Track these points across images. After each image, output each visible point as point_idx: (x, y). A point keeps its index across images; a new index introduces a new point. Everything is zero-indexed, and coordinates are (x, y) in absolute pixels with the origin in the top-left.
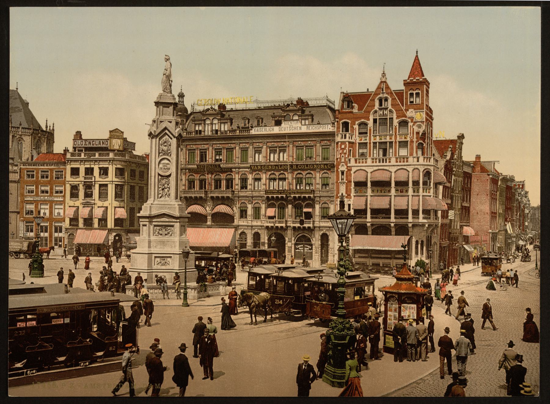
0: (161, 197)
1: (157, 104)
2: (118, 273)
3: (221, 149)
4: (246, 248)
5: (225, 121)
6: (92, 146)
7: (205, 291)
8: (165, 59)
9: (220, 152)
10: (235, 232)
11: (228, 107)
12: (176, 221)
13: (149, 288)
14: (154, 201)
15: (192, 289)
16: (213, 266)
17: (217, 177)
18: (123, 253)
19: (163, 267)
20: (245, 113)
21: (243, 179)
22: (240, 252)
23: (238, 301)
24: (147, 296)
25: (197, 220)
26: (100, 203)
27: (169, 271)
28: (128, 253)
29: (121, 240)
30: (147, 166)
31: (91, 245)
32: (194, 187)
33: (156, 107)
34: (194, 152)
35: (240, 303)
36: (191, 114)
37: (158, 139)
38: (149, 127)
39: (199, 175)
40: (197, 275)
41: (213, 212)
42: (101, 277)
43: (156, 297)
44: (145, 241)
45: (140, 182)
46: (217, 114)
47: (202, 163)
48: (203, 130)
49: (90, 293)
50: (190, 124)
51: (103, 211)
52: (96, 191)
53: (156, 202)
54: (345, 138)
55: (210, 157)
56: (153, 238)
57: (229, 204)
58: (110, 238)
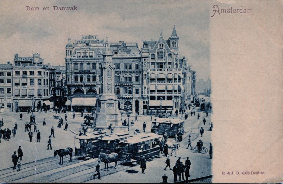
54: (146, 60)
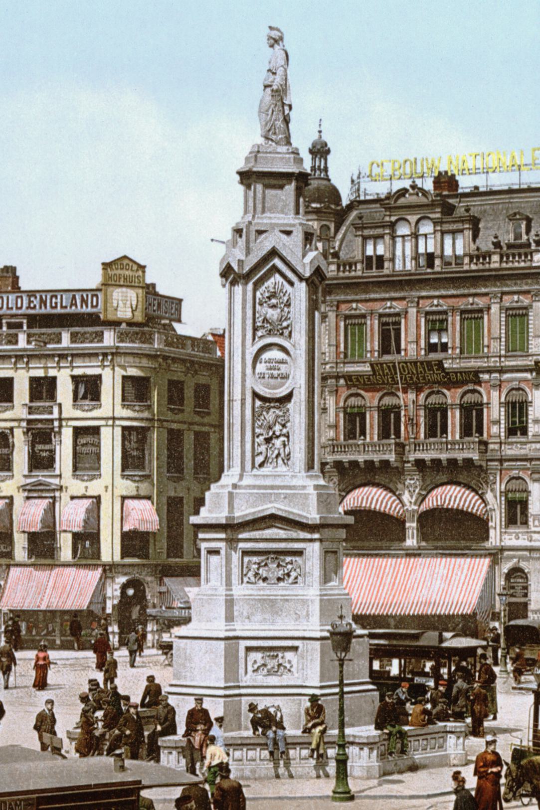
0: (262, 465)
1: (247, 177)
2: (136, 698)
3: (445, 313)
4: (526, 617)
5: (455, 227)
6: (49, 310)
7: (403, 752)
8: (270, 38)
9: (442, 321)
10: (492, 567)
11: (465, 183)
12: (309, 536)
13: (230, 745)
14: (241, 477)
15: (362, 745)
16: (426, 675)
17: (433, 399)
18: (149, 637)
19: (274, 680)
20: (517, 199)
21: (514, 404)
22: (507, 629)
23: (503, 781)
24: (223, 769)
25: (372, 533)
26: (76, 486)
27: (290, 692)
28: (166, 637)
29: (144, 597)
30: (218, 368)
31: (51, 614)
32: (363, 433)
33: (241, 188)
34: (361, 325)
35: (510, 788)
36: (351, 207)
37: (250, 286)
38: (221, 250)
39: (378, 395)
40: (377, 704)
41: (424, 508)
42: (84, 713)
43: (253, 771)
44: (216, 600)
45: (197, 419)
46: (431, 206)
47: (387, 358)
48: (388, 255)
49: (52, 763)
50: (350, 236)
51: (88, 511)
52: (64, 448)
53: (244, 482)
55: (412, 337)
56: (239, 590)
57: (473, 484)
58: (109, 594)
